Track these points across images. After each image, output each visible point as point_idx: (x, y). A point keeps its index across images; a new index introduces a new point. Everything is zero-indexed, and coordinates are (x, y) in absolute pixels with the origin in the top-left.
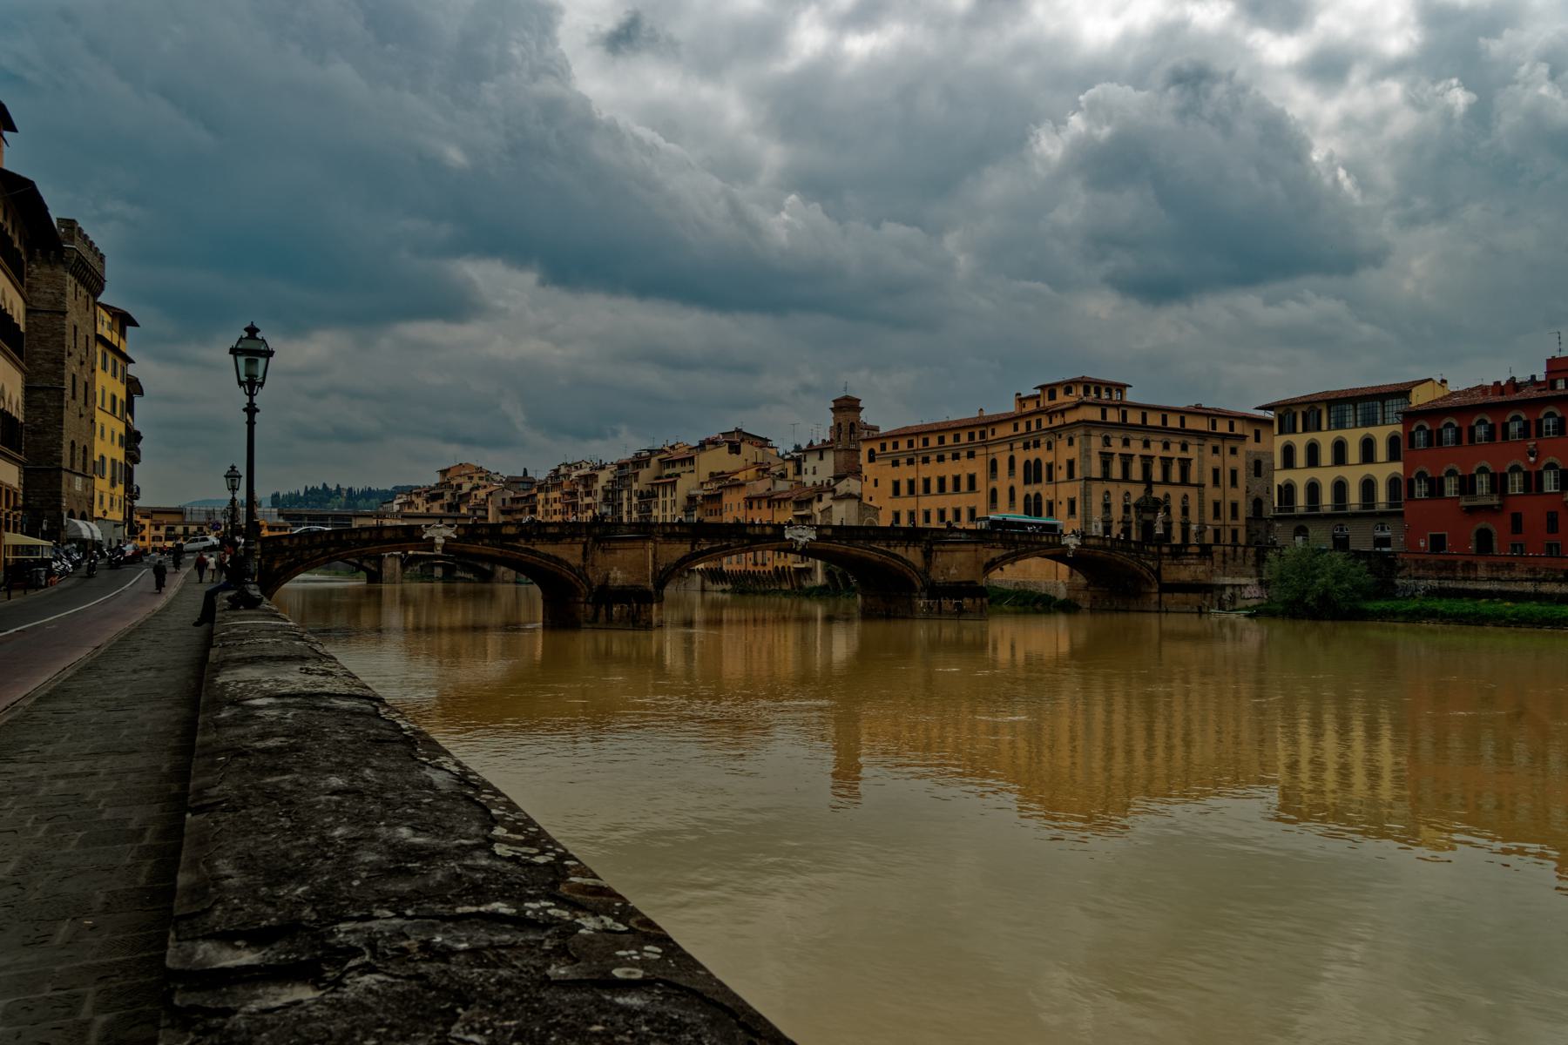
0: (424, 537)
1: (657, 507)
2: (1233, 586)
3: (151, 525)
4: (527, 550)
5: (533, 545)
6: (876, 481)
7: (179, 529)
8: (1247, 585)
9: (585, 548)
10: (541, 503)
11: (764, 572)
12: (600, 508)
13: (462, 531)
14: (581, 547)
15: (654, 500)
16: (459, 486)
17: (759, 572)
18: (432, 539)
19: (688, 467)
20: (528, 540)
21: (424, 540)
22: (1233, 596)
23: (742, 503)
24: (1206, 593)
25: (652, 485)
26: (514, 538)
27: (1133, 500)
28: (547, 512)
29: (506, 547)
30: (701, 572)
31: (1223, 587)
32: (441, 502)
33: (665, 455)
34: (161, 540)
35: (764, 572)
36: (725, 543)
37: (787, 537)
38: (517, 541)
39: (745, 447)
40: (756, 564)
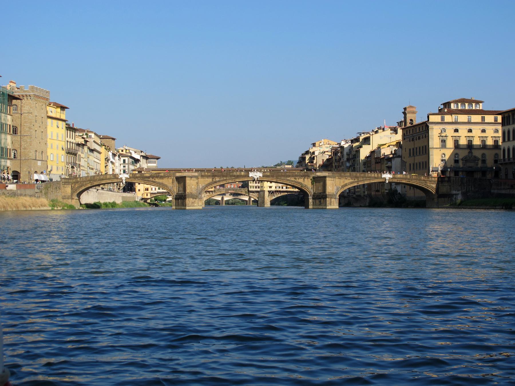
0: (119, 178)
2: (456, 194)
5: (155, 179)
6: (405, 148)
8: (459, 194)
9: (173, 180)
13: (131, 175)
14: (172, 180)
16: (314, 153)
18: (121, 178)
20: (153, 178)
21: (119, 179)
22: (455, 198)
24: (449, 198)
26: (149, 177)
27: (461, 157)
29: (146, 180)
31: (453, 195)
36: (225, 178)
37: (250, 175)
38: (149, 178)
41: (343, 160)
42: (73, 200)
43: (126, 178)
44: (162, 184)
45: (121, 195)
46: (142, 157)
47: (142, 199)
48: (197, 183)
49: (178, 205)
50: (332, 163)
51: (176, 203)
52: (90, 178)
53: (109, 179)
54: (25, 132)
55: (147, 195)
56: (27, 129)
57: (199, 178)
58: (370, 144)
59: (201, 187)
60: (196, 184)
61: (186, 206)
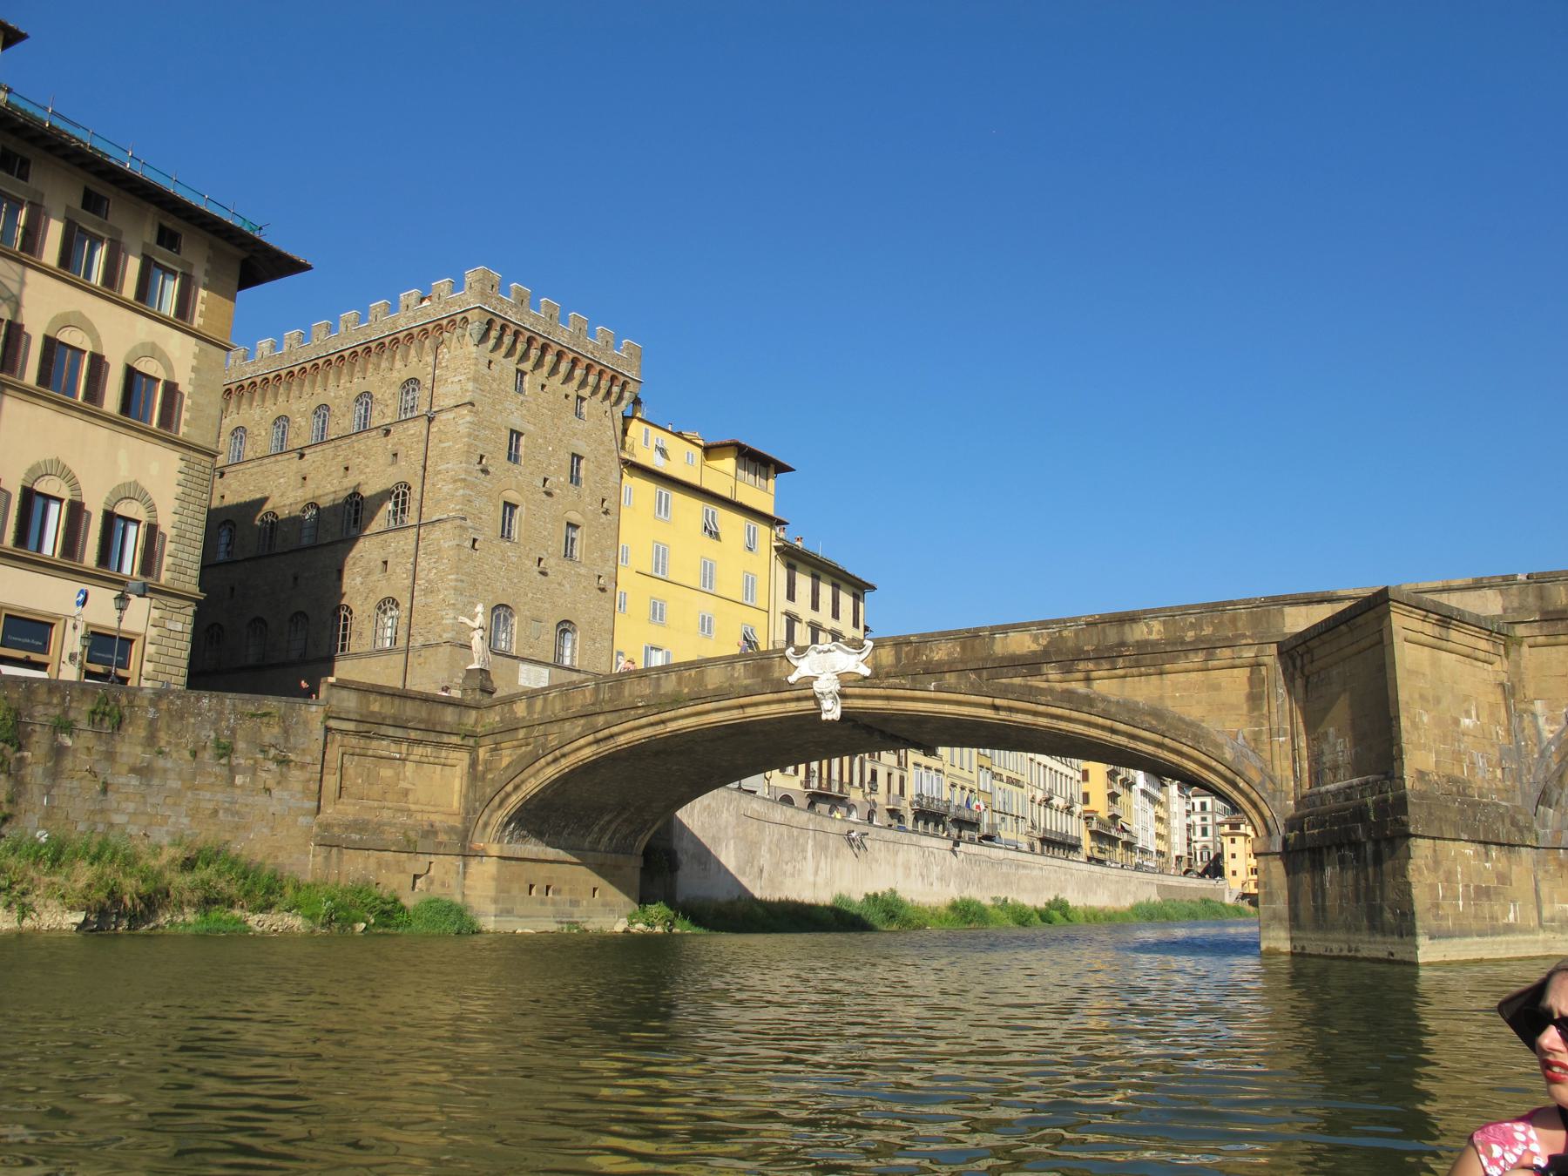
4: (1069, 698)
5: (1088, 680)
9: (1255, 681)
13: (887, 656)
20: (1067, 667)
26: (1030, 664)
29: (1005, 692)
42: (474, 862)
43: (845, 679)
44: (1157, 714)
45: (1156, 882)
47: (1244, 896)
48: (1509, 691)
49: (1321, 920)
51: (1293, 899)
52: (589, 698)
53: (719, 695)
54: (438, 502)
56: (445, 489)
57: (1519, 642)
59: (1548, 731)
60: (1498, 697)
61: (1405, 926)
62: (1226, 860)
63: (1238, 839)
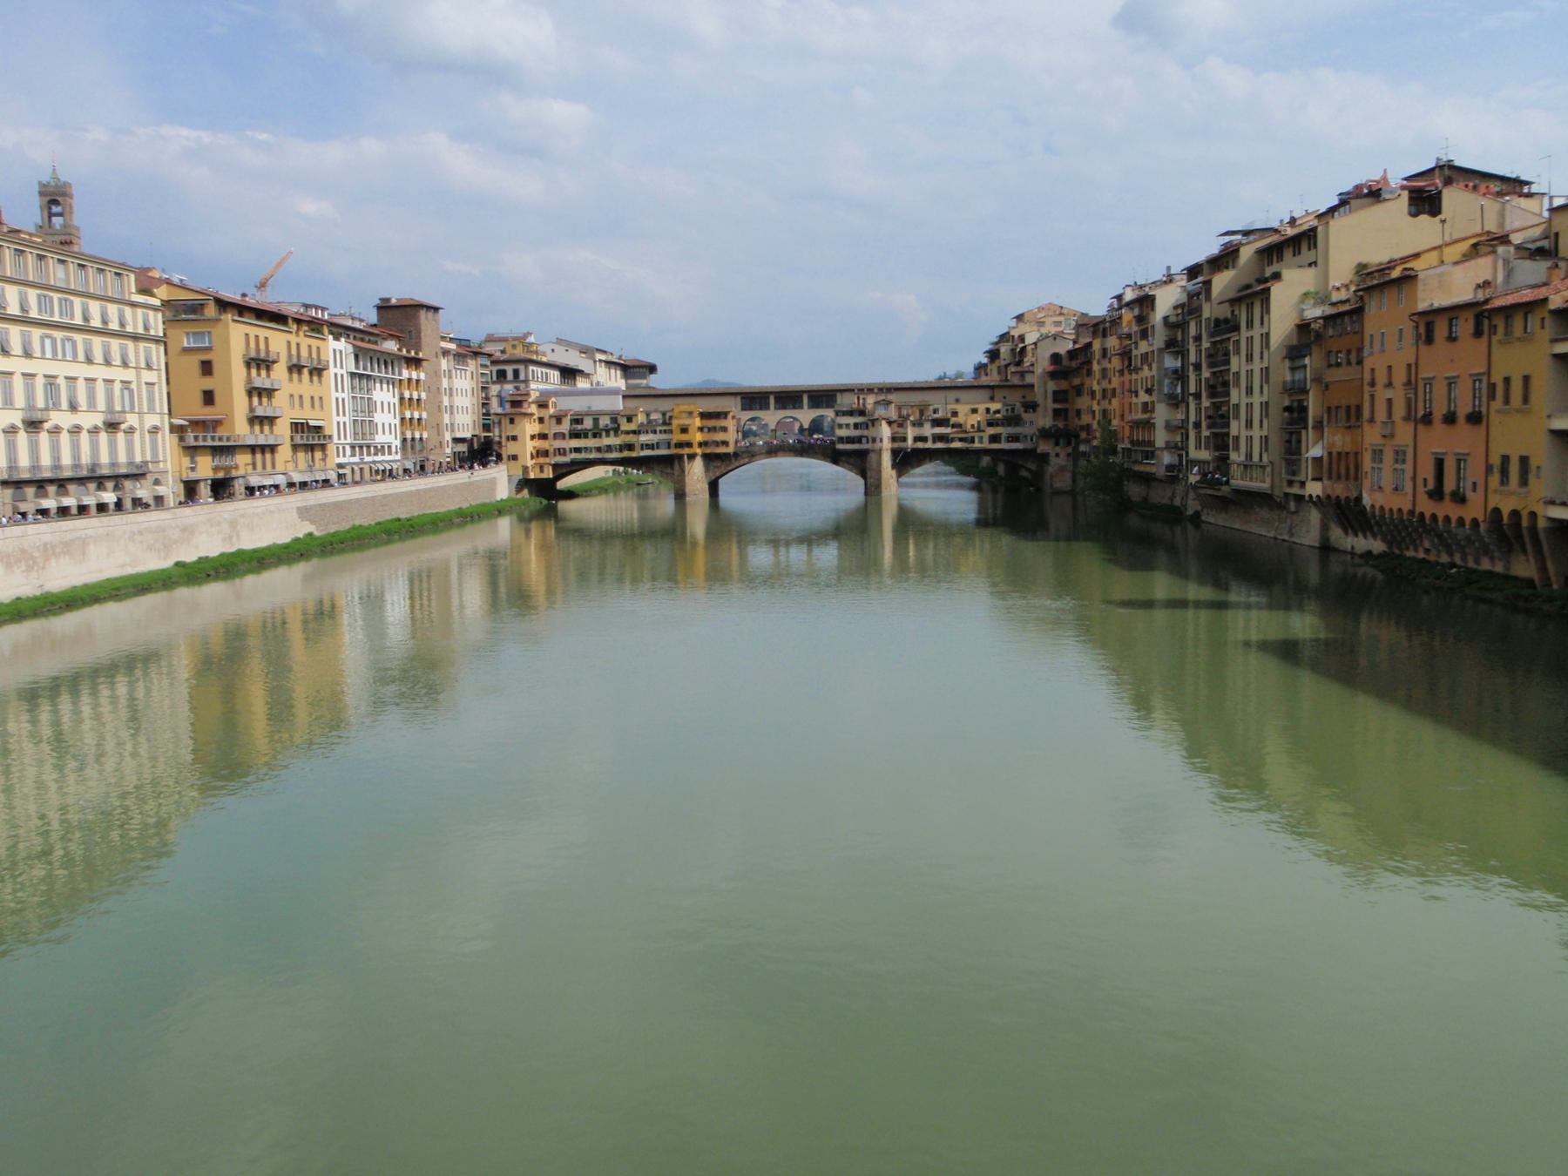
1: (1238, 352)
3: (551, 417)
7: (588, 423)
10: (1097, 358)
11: (1461, 521)
12: (1161, 362)
15: (1234, 337)
16: (1022, 338)
17: (1447, 519)
19: (1307, 255)
23: (1408, 326)
25: (1234, 302)
28: (1104, 370)
30: (1318, 502)
32: (997, 363)
33: (1275, 238)
34: (564, 438)
35: (1461, 521)
39: (1454, 199)
40: (1437, 494)
41: (1152, 345)
46: (603, 364)
50: (1089, 362)
55: (542, 471)
58: (1315, 263)
62: (503, 444)
63: (517, 419)
